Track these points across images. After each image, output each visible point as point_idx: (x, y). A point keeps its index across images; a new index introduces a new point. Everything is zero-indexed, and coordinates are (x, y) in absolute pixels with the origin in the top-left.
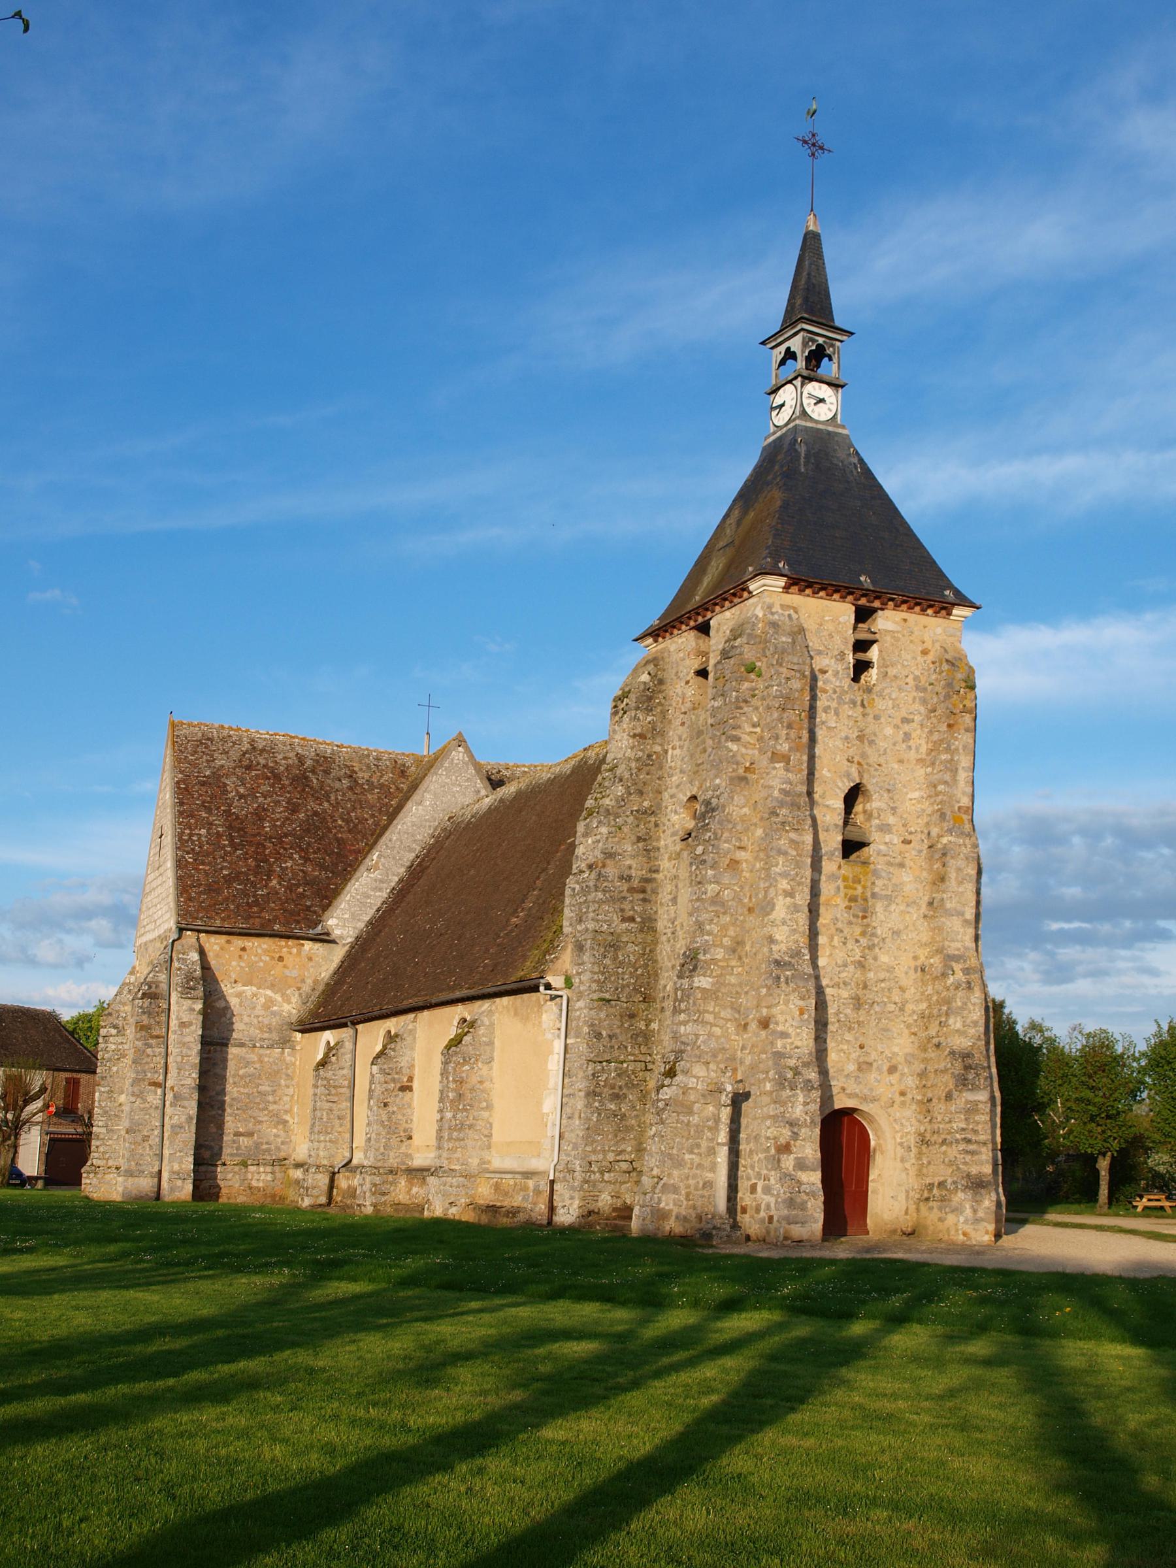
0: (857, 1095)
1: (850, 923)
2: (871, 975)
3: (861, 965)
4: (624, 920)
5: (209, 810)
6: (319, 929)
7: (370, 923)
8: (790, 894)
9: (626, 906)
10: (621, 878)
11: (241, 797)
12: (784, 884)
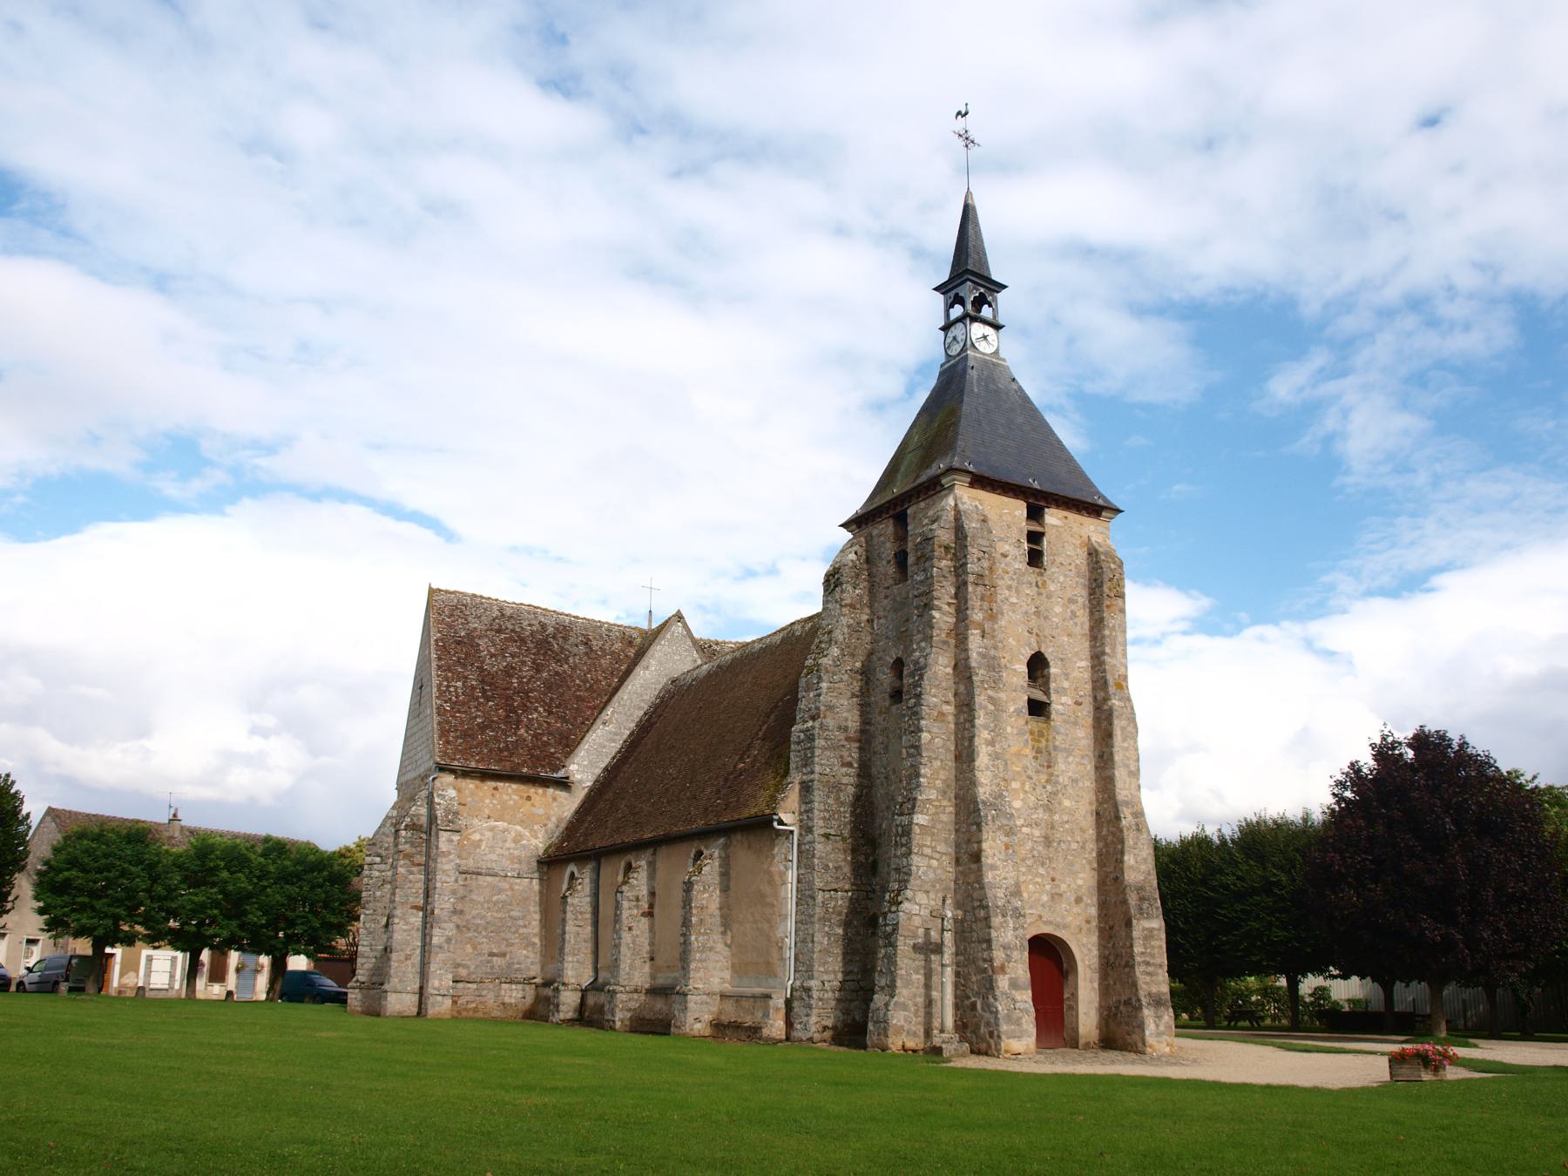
0: (1050, 923)
1: (1038, 772)
2: (1057, 817)
3: (1048, 808)
4: (843, 765)
5: (464, 666)
6: (561, 774)
7: (606, 769)
8: (991, 743)
9: (845, 754)
10: (840, 728)
11: (492, 656)
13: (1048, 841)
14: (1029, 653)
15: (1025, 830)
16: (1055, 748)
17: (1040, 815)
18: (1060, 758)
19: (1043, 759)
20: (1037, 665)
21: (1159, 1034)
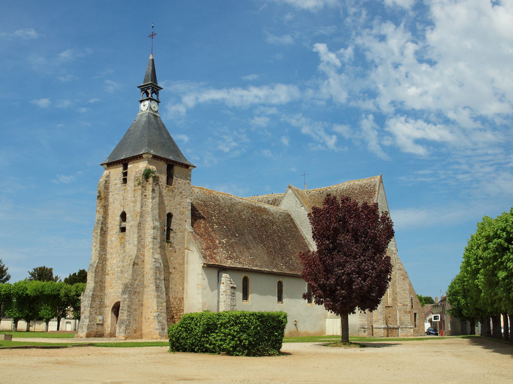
2: (125, 264)
3: (123, 261)
8: (95, 246)
12: (94, 244)
13: (122, 272)
14: (120, 213)
15: (116, 269)
16: (126, 241)
18: (127, 244)
20: (123, 216)
21: (120, 333)
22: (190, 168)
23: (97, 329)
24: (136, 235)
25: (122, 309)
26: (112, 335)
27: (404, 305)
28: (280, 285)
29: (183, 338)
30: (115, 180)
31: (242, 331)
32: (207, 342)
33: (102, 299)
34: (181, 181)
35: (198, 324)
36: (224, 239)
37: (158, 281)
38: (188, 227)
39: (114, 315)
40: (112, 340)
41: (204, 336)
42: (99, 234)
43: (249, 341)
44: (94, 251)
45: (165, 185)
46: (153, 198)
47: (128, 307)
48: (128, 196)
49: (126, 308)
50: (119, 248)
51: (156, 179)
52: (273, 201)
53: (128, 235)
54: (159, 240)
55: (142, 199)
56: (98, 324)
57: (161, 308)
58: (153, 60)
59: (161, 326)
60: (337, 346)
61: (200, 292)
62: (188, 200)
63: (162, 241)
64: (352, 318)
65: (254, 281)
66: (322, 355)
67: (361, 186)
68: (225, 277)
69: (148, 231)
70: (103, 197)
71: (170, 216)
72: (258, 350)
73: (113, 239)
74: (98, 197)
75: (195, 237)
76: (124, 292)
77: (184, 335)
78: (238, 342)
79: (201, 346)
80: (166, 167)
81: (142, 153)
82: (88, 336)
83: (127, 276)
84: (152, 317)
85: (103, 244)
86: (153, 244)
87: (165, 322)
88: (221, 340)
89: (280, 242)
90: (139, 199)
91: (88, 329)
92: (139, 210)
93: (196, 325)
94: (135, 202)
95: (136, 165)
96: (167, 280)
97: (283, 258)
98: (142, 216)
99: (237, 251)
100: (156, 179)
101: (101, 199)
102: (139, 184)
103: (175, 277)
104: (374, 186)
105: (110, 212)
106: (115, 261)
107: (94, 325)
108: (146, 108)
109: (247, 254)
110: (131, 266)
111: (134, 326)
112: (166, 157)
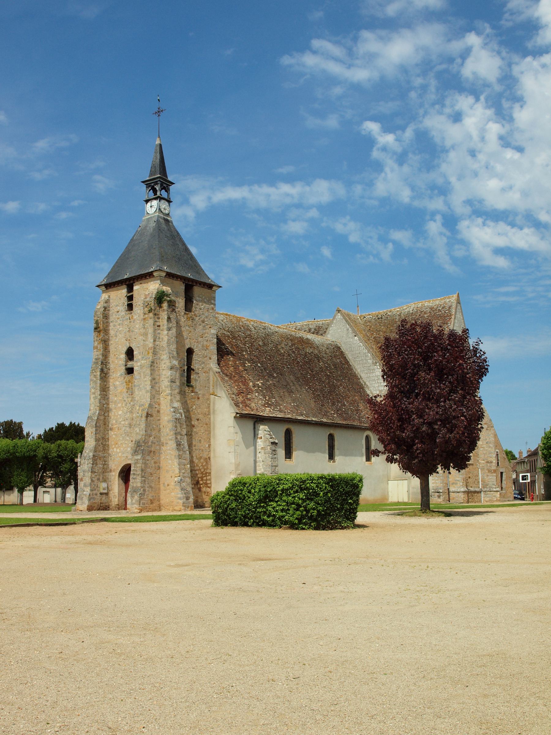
2: (134, 415)
3: (131, 412)
8: (94, 393)
12: (93, 391)
13: (130, 425)
14: (125, 349)
15: (123, 423)
16: (135, 386)
17: (128, 415)
19: (130, 393)
20: (130, 354)
21: (133, 504)
22: (214, 288)
23: (101, 499)
24: (148, 378)
25: (134, 474)
26: (123, 506)
27: (488, 462)
28: (331, 438)
29: (232, 509)
30: (117, 306)
31: (308, 499)
32: (265, 513)
33: (105, 462)
34: (203, 306)
35: (253, 491)
36: (259, 380)
37: (179, 437)
38: (213, 365)
39: (121, 482)
40: (123, 514)
41: (260, 506)
42: (99, 377)
43: (318, 511)
44: (92, 400)
45: (183, 311)
46: (169, 329)
47: (142, 470)
48: (135, 326)
49: (139, 472)
50: (125, 395)
51: (172, 304)
52: (315, 329)
53: (137, 377)
54: (178, 383)
55: (155, 331)
56: (101, 494)
57: (183, 471)
58: (161, 145)
59: (185, 494)
60: (415, 515)
61: (232, 450)
62: (213, 331)
63: (182, 384)
64: (434, 481)
65: (298, 434)
66: (396, 526)
67: (431, 308)
68: (263, 429)
69: (164, 372)
70: (101, 329)
71: (190, 352)
72: (329, 522)
73: (118, 383)
74: (95, 329)
75: (223, 379)
76: (135, 452)
77: (234, 505)
78: (305, 513)
79: (257, 518)
80: (184, 288)
81: (152, 270)
82: (90, 509)
83: (139, 432)
84: (173, 484)
85: (104, 390)
86: (171, 390)
87: (189, 489)
88: (282, 510)
89: (329, 383)
90: (151, 330)
91: (89, 500)
92: (151, 345)
93: (250, 492)
94: (145, 334)
95: (145, 285)
96: (189, 435)
97: (333, 404)
98: (155, 353)
99: (276, 396)
100: (172, 304)
101: (99, 332)
102: (150, 311)
103: (199, 430)
104: (450, 308)
105: (112, 348)
106: (120, 413)
107: (96, 494)
108: (154, 209)
109: (289, 400)
110: (144, 419)
111: (150, 495)
112: (184, 274)
